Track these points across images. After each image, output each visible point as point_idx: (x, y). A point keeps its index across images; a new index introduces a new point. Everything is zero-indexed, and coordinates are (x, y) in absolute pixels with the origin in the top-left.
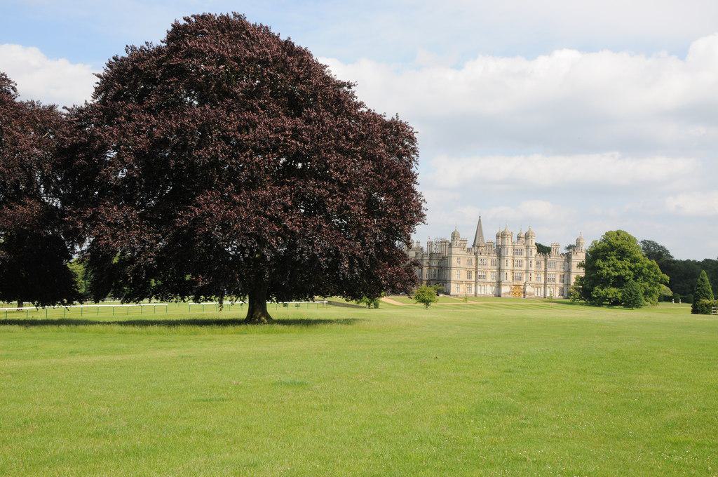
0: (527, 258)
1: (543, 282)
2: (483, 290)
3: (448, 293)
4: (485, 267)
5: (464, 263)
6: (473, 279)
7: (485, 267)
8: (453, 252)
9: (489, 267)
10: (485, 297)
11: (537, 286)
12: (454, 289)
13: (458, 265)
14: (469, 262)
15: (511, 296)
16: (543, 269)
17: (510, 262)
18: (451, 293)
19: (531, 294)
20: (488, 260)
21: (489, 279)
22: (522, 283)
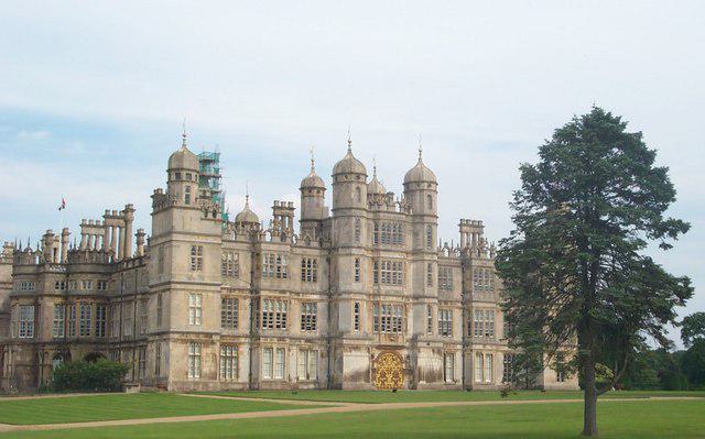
2: (277, 368)
6: (244, 325)
7: (284, 285)
9: (296, 284)
12: (178, 362)
16: (457, 293)
17: (366, 266)
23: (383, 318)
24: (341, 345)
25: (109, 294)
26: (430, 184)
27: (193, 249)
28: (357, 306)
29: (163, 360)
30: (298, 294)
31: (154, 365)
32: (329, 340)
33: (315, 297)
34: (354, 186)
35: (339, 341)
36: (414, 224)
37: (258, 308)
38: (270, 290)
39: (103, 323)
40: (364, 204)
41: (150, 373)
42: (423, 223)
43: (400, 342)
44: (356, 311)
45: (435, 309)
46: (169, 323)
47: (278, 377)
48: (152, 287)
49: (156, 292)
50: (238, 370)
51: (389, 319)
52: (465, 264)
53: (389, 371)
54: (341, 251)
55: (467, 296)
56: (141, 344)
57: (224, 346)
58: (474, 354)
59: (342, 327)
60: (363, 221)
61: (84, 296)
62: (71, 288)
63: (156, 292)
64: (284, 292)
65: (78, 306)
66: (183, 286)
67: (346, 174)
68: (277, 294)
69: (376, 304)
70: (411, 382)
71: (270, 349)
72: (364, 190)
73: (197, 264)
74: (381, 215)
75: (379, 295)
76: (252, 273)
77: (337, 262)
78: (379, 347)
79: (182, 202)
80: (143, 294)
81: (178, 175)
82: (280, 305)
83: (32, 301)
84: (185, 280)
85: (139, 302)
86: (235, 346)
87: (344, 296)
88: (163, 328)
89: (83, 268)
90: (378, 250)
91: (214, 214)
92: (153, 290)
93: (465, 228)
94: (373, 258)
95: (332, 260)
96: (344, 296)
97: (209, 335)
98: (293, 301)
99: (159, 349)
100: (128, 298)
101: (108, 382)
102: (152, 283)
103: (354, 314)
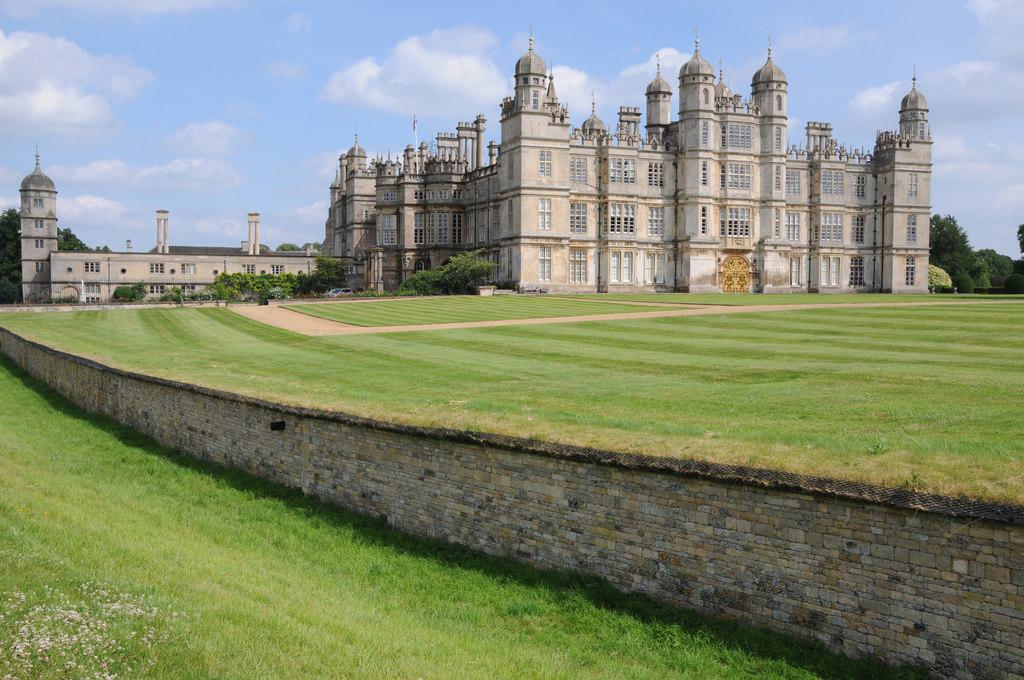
0: (765, 157)
1: (804, 241)
2: (625, 272)
3: (511, 284)
4: (631, 189)
5: (560, 174)
6: (592, 231)
7: (631, 189)
8: (526, 131)
10: (632, 297)
11: (791, 256)
12: (530, 266)
13: (544, 181)
14: (577, 169)
15: (719, 288)
16: (804, 198)
17: (714, 170)
18: (523, 283)
19: (778, 280)
20: (639, 162)
21: (643, 232)
22: (750, 243)
23: (730, 222)
24: (689, 249)
25: (464, 203)
26: (780, 83)
27: (542, 154)
28: (704, 210)
29: (514, 263)
30: (645, 198)
31: (507, 268)
32: (675, 242)
34: (702, 87)
35: (685, 244)
36: (762, 126)
37: (606, 213)
38: (617, 195)
39: (460, 230)
40: (712, 106)
41: (503, 276)
42: (772, 125)
43: (747, 246)
44: (704, 215)
45: (783, 211)
46: (519, 229)
47: (625, 280)
48: (502, 193)
49: (506, 198)
50: (586, 273)
51: (736, 222)
52: (813, 167)
53: (736, 274)
54: (687, 154)
55: (815, 199)
56: (494, 249)
57: (573, 250)
58: (821, 258)
59: (688, 231)
60: (711, 124)
61: (442, 205)
62: (430, 198)
63: (506, 198)
64: (631, 196)
65: (436, 216)
66: (532, 192)
68: (624, 199)
69: (723, 208)
70: (757, 286)
71: (617, 254)
72: (711, 90)
73: (545, 169)
74: (730, 118)
75: (727, 199)
76: (600, 178)
77: (683, 165)
78: (726, 251)
79: (529, 108)
80: (495, 201)
81: (526, 81)
82: (627, 209)
83: (394, 210)
84: (535, 186)
85: (491, 210)
86: (583, 250)
87: (691, 200)
88: (514, 233)
89: (439, 178)
90: (726, 154)
91: (562, 118)
92: (504, 196)
93: (812, 132)
94: (720, 162)
95: (679, 166)
96: (691, 200)
97: (560, 239)
98: (640, 206)
99: (510, 253)
100: (482, 206)
101: (464, 285)
102: (503, 188)
103: (701, 218)
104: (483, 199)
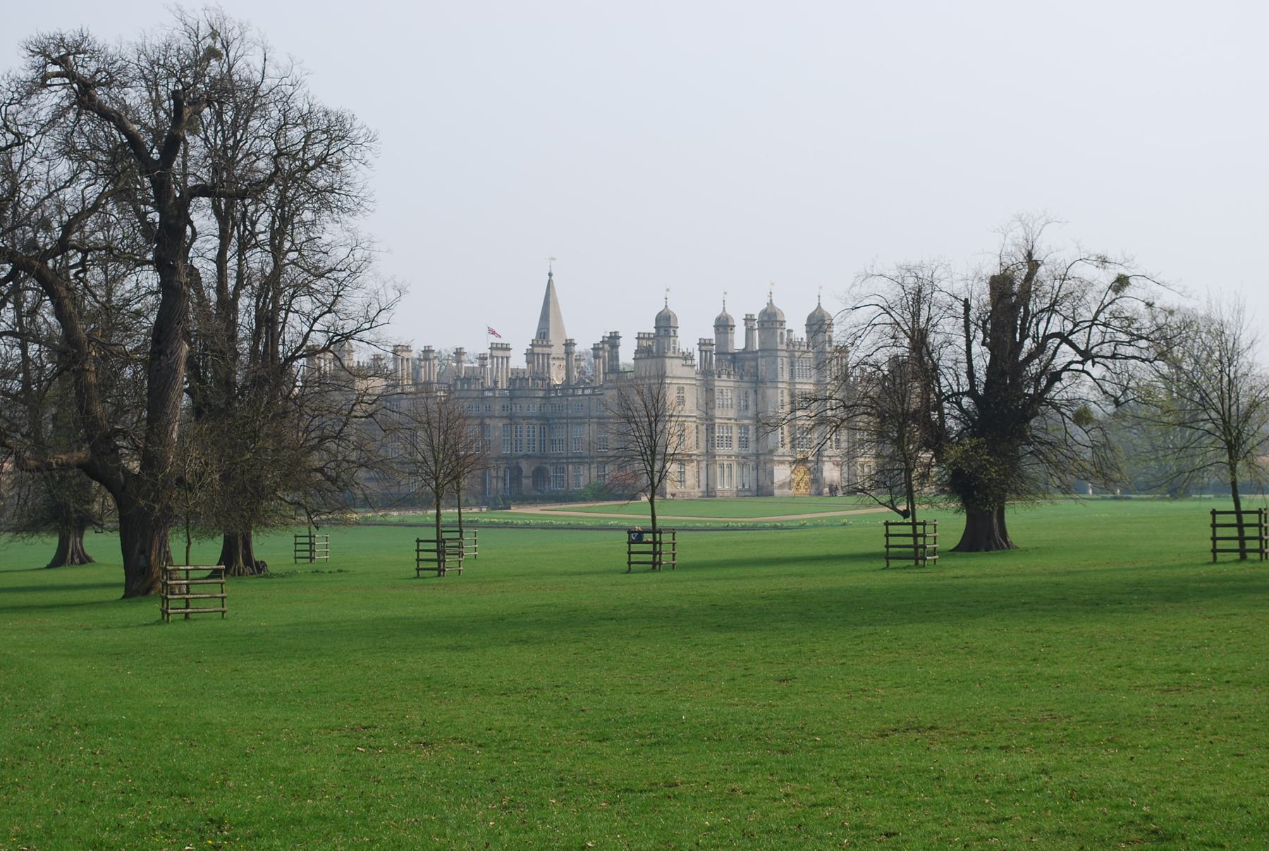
32: (757, 455)
33: (746, 422)
37: (713, 432)
62: (516, 410)
67: (769, 320)
79: (670, 354)
83: (478, 421)
104: (581, 414)
